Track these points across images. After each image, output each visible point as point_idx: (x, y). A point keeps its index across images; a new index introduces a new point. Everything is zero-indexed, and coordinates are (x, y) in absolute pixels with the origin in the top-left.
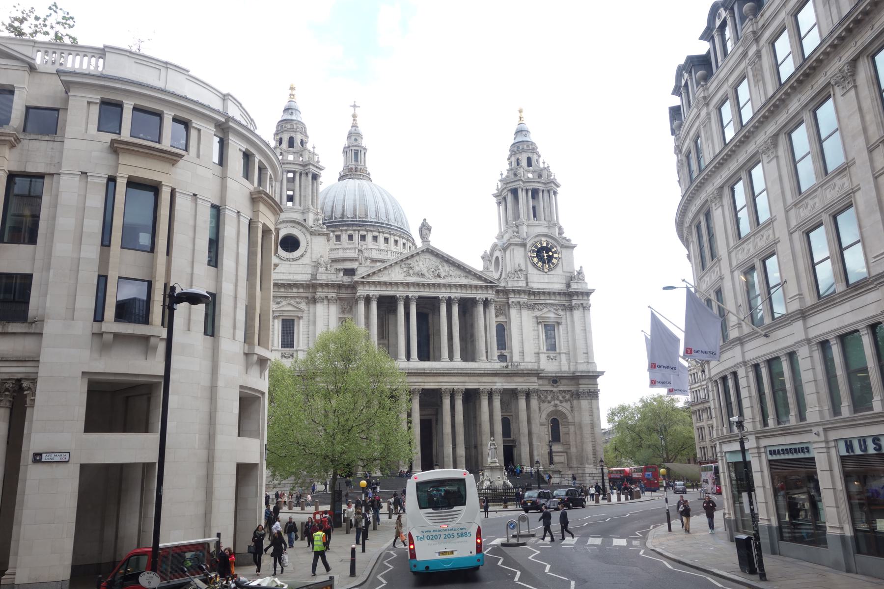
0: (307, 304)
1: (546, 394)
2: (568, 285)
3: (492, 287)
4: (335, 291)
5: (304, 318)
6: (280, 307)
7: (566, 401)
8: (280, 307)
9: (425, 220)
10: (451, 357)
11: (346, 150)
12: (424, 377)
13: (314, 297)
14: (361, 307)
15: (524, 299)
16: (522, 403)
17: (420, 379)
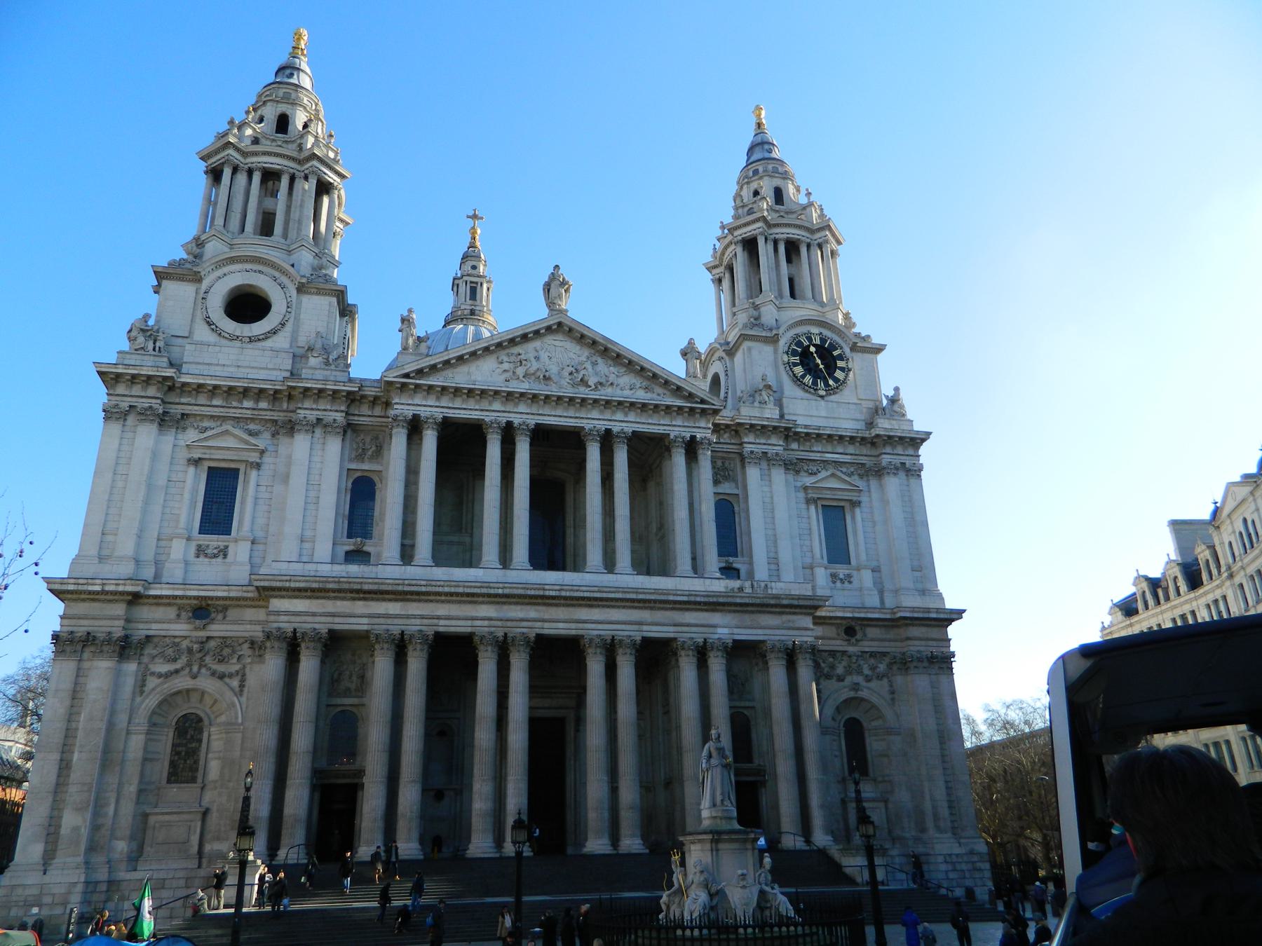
0: (273, 436)
1: (831, 660)
2: (870, 425)
3: (703, 411)
4: (343, 408)
5: (264, 467)
6: (206, 439)
7: (880, 677)
8: (206, 439)
9: (557, 267)
10: (609, 564)
11: (456, 282)
12: (544, 608)
13: (290, 421)
14: (399, 441)
15: (776, 445)
16: (777, 673)
17: (532, 612)
